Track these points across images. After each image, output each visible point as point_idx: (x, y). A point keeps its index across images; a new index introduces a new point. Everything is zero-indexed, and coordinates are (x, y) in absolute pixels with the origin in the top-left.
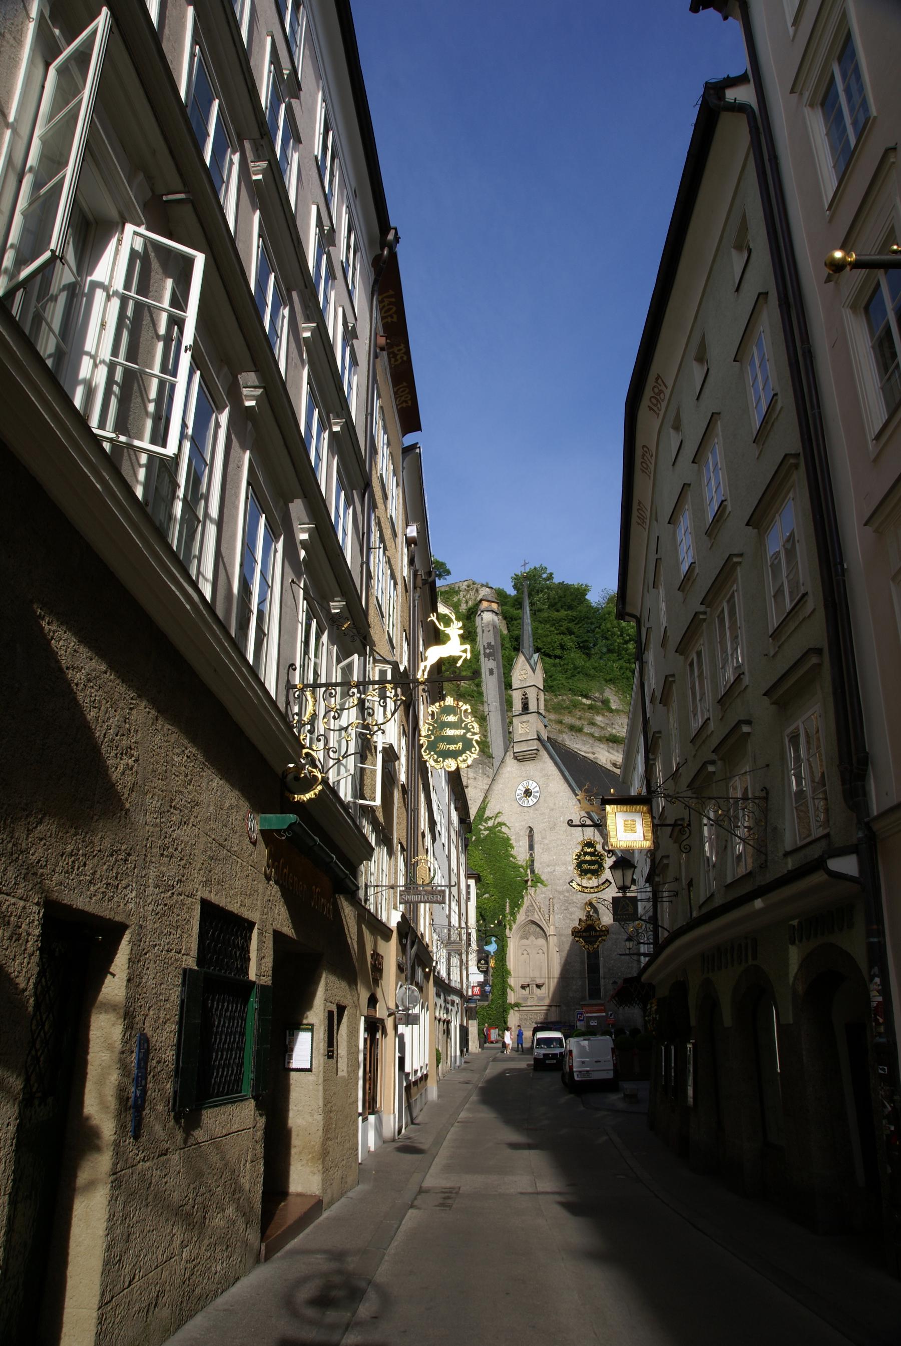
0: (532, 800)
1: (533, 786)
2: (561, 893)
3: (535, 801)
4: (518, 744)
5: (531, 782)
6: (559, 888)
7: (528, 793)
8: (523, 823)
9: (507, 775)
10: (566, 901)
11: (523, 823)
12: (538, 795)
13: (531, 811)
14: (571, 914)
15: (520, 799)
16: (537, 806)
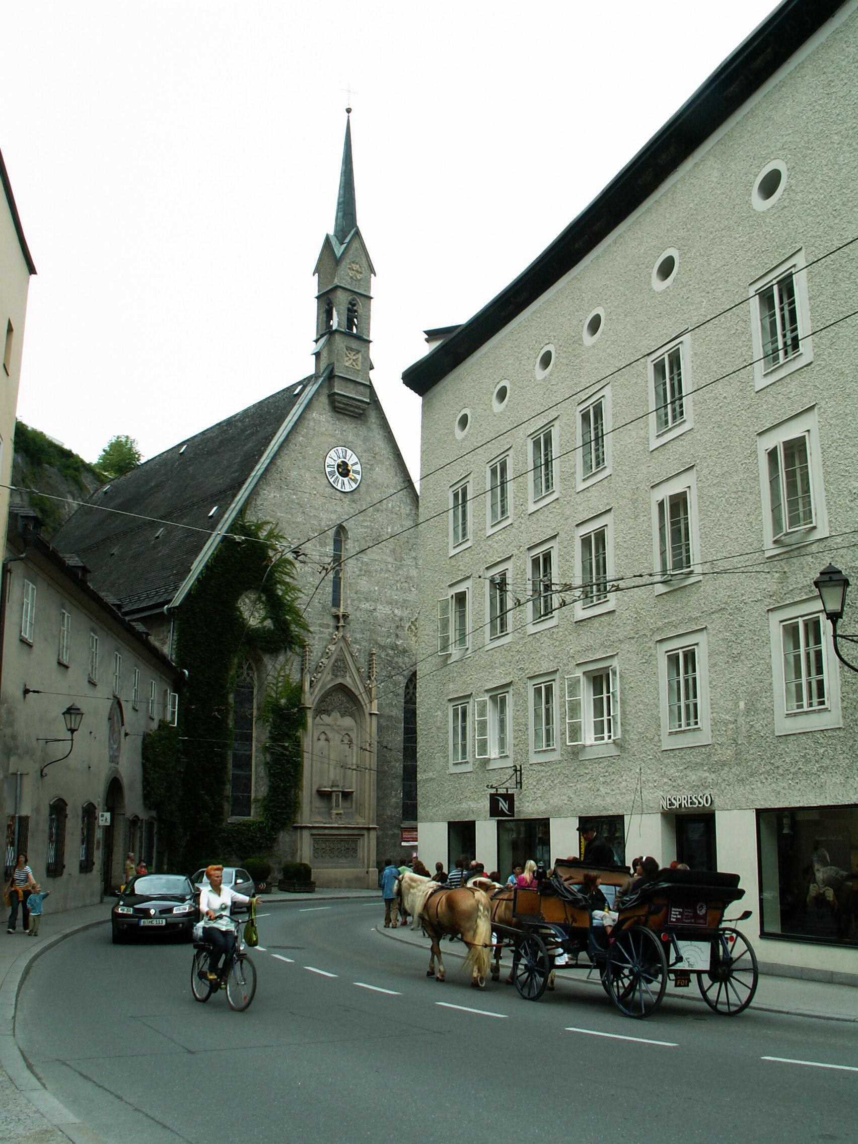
0: (348, 486)
1: (352, 459)
2: (382, 647)
3: (355, 486)
4: (343, 383)
5: (349, 452)
6: (382, 641)
7: (344, 470)
8: (334, 517)
9: (312, 424)
10: (390, 663)
11: (334, 517)
12: (359, 477)
13: (346, 500)
14: (396, 684)
15: (332, 474)
16: (356, 496)
